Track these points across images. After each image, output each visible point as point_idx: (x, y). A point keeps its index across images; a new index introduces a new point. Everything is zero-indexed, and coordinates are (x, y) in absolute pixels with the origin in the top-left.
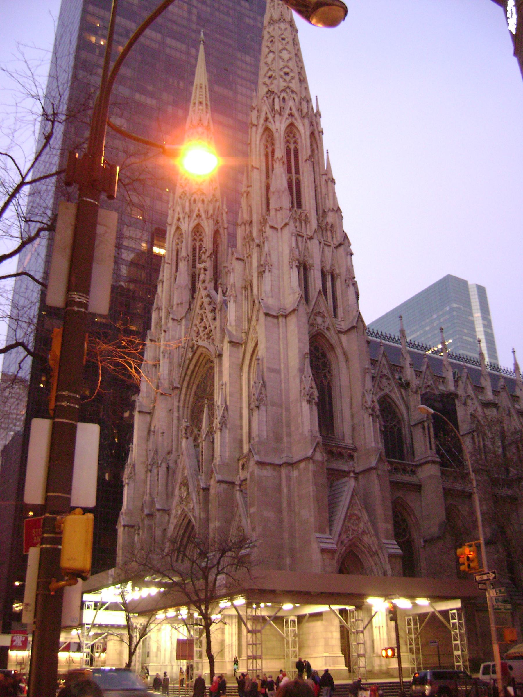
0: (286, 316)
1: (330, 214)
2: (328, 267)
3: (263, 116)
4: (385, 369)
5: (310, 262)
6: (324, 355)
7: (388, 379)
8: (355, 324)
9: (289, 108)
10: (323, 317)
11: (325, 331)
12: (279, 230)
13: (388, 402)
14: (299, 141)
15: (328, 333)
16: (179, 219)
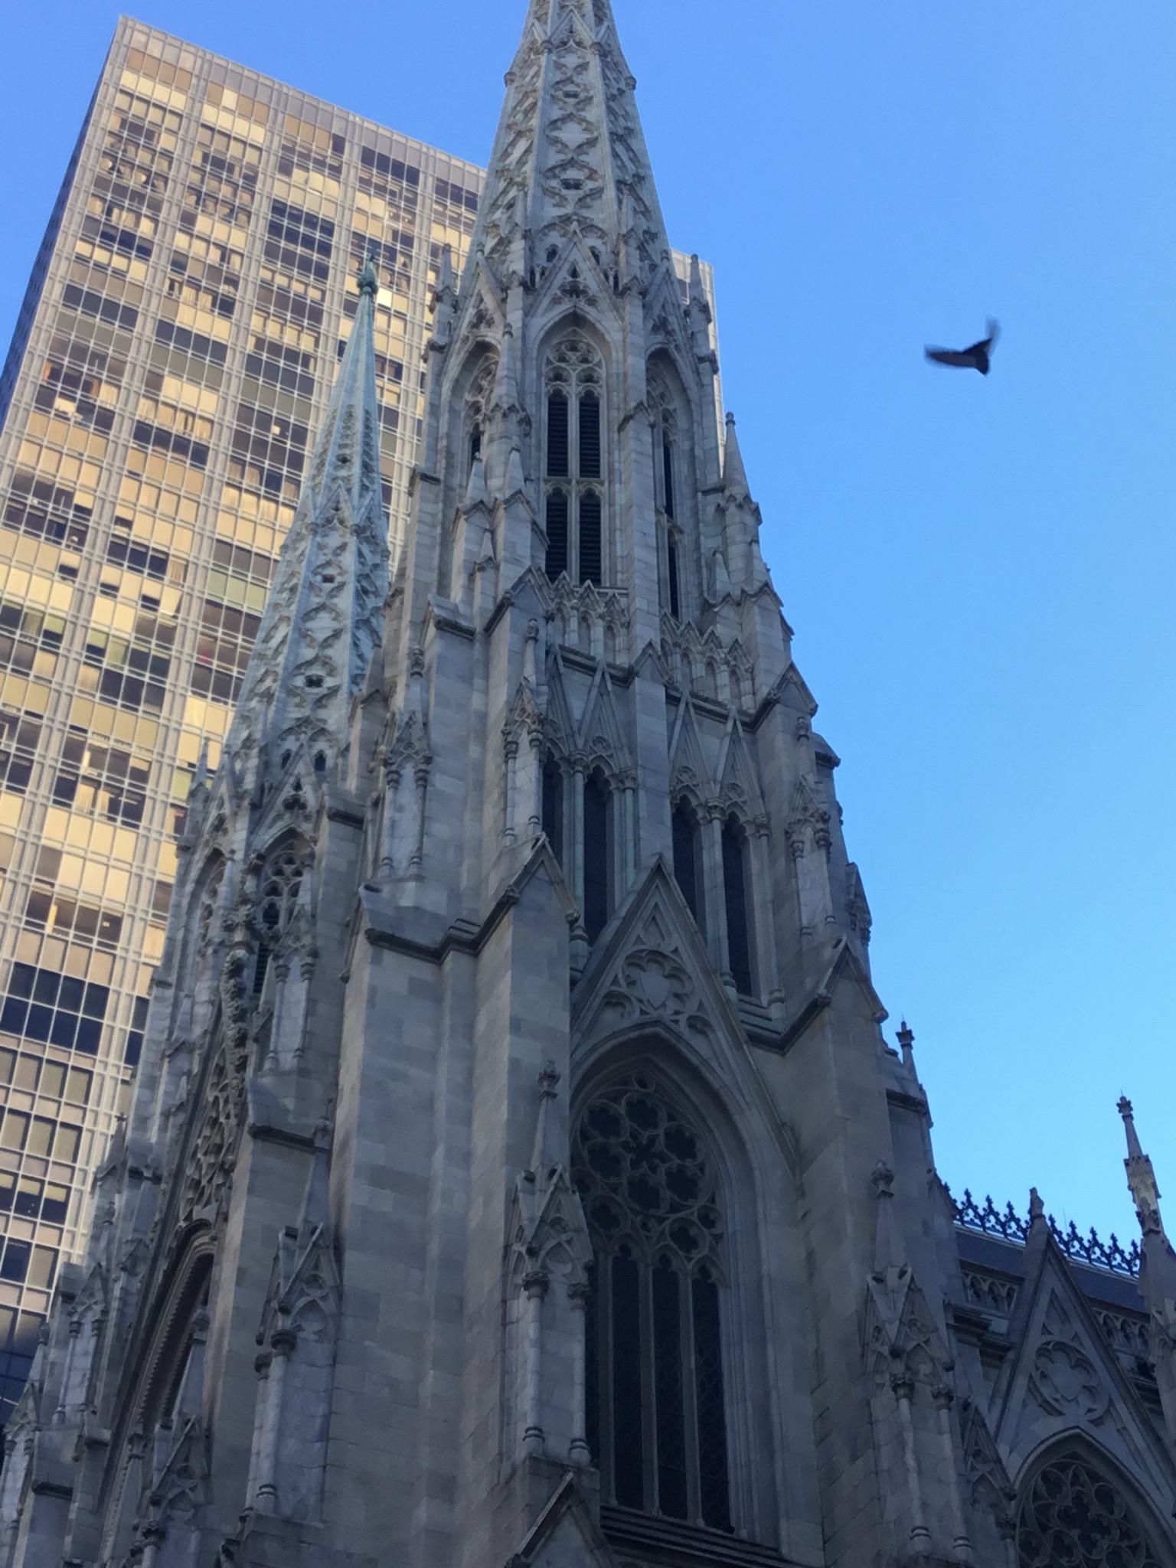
0: (474, 947)
1: (728, 611)
2: (709, 793)
3: (470, 313)
4: (1065, 1318)
5: (622, 760)
6: (683, 1144)
7: (1081, 1364)
8: (822, 990)
9: (567, 266)
10: (676, 974)
11: (683, 1028)
12: (478, 637)
13: (1095, 1477)
14: (602, 372)
15: (699, 1043)
16: (221, 822)
